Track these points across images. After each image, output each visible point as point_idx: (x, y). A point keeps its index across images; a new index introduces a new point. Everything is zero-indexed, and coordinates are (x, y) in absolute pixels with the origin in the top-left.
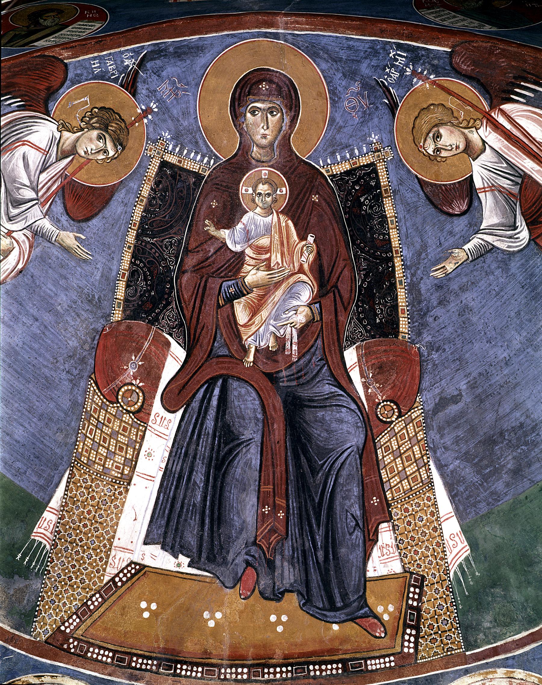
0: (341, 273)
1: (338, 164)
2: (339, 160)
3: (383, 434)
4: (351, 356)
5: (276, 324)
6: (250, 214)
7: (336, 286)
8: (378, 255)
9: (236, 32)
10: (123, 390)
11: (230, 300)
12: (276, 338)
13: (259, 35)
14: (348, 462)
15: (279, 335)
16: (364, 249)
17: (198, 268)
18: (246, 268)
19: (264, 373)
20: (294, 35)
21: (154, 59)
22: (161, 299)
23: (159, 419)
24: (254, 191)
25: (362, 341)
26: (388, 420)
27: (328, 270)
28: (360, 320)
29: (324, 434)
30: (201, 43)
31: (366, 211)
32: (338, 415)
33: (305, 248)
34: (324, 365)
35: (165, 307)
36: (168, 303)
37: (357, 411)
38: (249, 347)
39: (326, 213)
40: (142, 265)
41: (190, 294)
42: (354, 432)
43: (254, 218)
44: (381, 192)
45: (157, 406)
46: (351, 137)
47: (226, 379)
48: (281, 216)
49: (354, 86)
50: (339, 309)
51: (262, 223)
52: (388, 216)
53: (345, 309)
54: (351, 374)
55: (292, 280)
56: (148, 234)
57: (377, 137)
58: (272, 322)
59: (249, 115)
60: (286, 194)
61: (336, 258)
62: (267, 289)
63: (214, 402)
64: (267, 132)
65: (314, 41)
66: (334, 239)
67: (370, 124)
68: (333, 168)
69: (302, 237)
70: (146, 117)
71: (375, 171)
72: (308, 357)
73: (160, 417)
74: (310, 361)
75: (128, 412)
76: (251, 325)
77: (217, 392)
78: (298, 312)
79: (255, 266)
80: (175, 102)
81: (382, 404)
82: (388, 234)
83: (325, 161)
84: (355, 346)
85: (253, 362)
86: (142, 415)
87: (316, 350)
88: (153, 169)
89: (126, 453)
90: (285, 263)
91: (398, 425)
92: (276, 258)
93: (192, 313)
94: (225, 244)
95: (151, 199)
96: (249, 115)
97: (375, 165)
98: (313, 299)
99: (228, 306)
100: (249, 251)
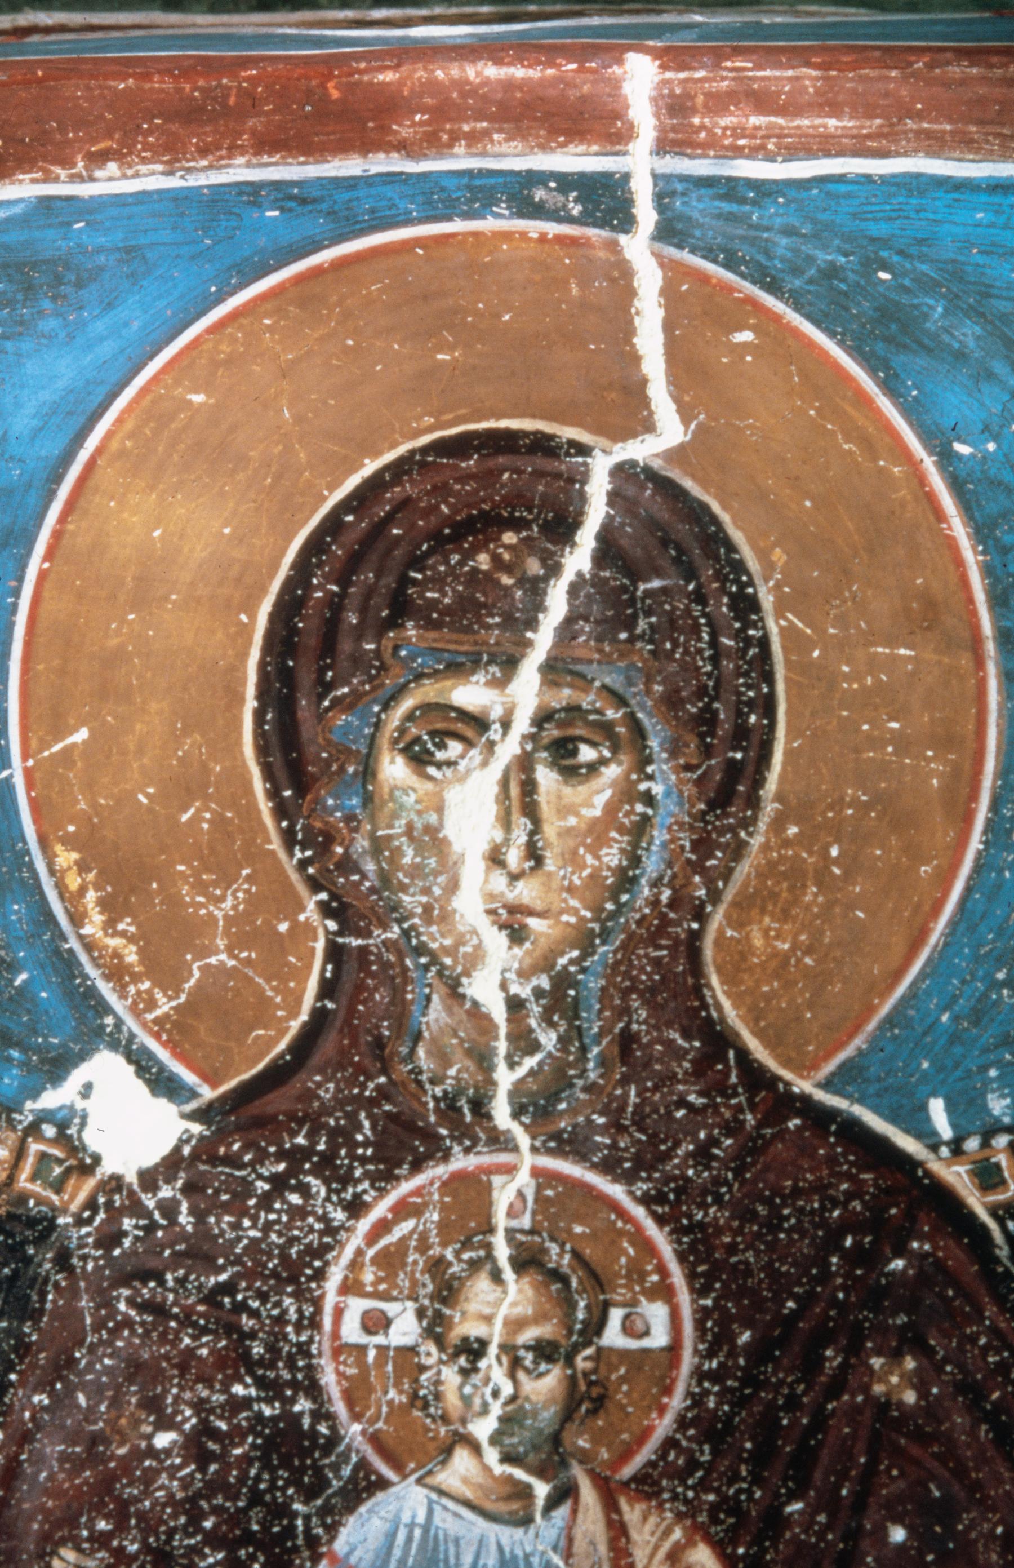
6: (406, 1501)
9: (312, 171)
13: (480, 192)
20: (730, 189)
24: (435, 1328)
30: (51, 242)
48: (631, 1513)
59: (394, 769)
60: (674, 1349)
64: (526, 892)
65: (875, 229)
83: (965, 1106)
96: (394, 769)
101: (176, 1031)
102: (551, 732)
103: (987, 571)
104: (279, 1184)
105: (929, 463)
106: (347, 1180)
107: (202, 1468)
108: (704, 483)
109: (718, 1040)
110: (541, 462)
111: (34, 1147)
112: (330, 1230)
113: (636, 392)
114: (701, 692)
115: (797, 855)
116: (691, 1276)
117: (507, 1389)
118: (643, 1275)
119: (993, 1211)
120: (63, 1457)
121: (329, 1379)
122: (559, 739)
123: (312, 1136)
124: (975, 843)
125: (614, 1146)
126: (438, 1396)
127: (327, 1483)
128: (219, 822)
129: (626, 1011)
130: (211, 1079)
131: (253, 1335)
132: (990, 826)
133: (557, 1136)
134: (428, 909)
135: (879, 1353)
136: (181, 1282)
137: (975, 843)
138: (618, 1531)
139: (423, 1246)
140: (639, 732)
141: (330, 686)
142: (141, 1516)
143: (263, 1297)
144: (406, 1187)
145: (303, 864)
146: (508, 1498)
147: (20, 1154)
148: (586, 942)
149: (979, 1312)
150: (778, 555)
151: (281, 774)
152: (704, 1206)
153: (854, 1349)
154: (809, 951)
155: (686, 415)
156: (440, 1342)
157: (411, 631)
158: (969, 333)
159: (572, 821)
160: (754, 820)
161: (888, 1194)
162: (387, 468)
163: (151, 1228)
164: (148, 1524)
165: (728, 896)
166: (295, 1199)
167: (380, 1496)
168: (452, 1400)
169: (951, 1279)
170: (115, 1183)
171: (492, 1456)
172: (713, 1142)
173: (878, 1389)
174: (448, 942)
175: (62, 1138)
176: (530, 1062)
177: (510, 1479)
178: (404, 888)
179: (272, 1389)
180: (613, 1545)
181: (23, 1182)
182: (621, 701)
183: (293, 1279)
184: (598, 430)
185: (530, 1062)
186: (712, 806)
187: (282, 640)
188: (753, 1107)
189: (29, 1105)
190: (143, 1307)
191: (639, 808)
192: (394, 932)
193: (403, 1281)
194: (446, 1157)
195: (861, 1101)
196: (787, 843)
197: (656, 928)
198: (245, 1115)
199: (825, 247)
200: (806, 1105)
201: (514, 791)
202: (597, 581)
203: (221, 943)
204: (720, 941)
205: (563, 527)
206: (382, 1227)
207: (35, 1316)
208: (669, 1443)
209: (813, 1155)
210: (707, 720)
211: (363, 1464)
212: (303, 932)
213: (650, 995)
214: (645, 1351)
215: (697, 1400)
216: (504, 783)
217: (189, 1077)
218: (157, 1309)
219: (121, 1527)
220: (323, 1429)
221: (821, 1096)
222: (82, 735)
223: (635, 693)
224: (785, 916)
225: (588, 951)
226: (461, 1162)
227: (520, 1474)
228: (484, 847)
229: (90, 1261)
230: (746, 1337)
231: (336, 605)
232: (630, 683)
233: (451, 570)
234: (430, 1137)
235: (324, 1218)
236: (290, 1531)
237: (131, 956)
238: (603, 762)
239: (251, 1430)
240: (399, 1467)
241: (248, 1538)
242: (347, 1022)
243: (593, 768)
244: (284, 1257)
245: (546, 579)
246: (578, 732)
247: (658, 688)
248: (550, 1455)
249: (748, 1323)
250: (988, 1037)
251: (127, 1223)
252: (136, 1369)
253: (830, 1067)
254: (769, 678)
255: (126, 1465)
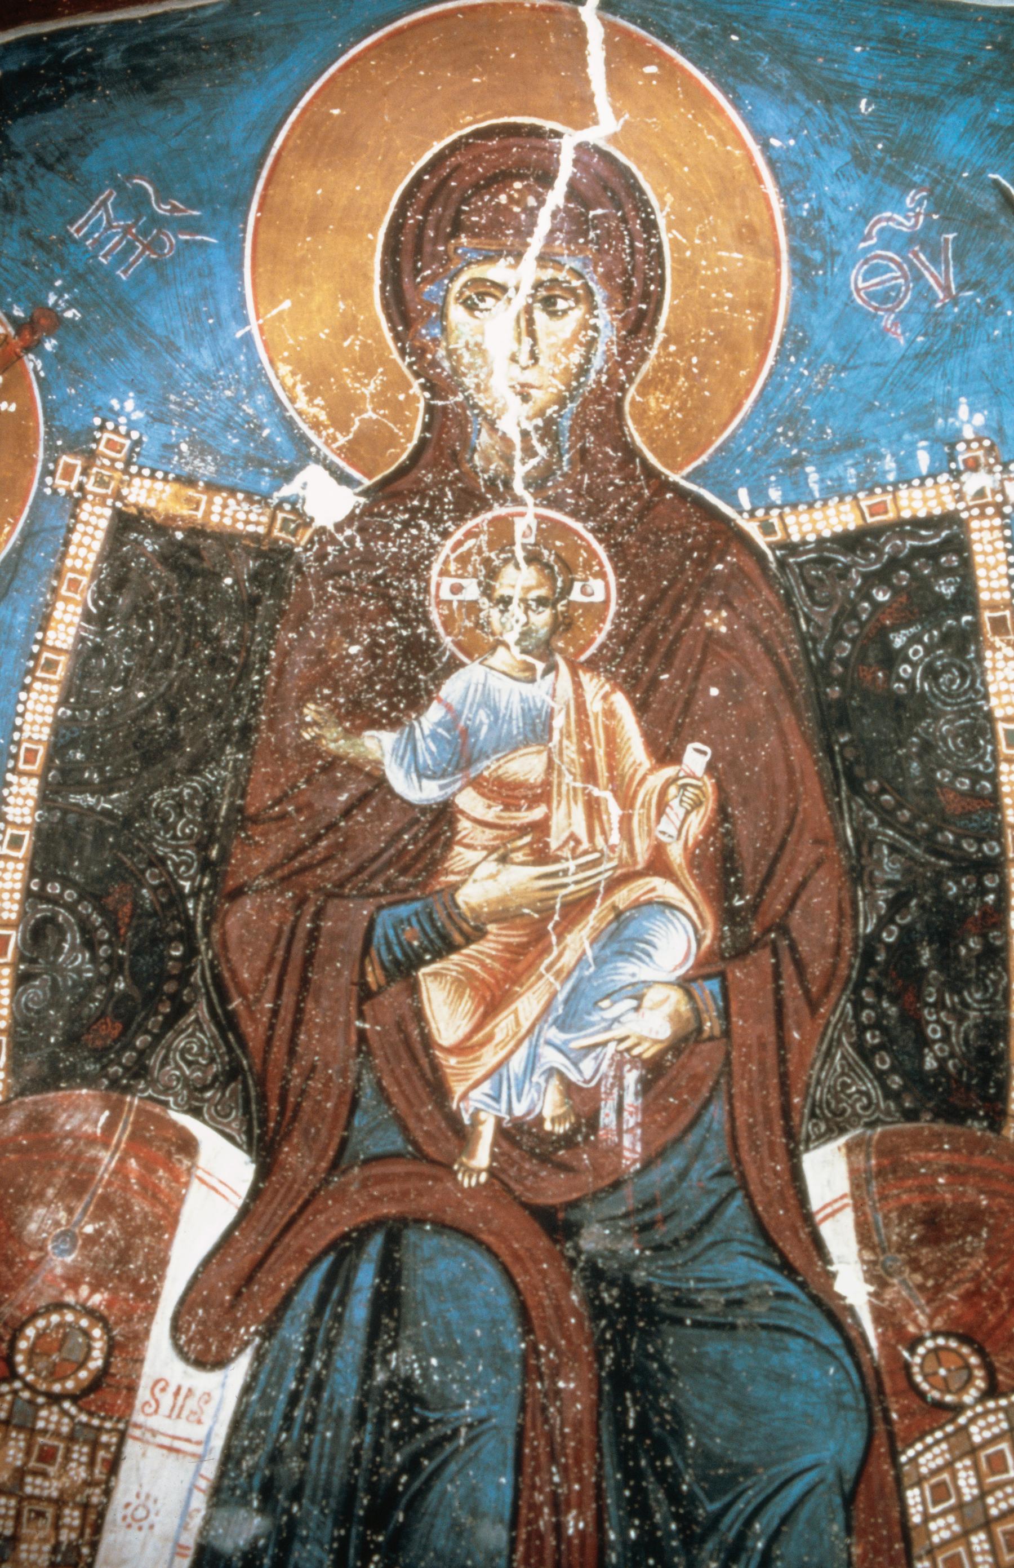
0: (802, 886)
1: (811, 506)
2: (815, 488)
3: (929, 1440)
4: (827, 1172)
5: (566, 1042)
7: (783, 930)
8: (946, 844)
10: (30, 1332)
11: (404, 969)
12: (569, 1089)
14: (804, 1513)
15: (574, 1076)
16: (891, 812)
17: (288, 873)
18: (461, 857)
19: (525, 1206)
21: (45, 105)
22: (151, 999)
23: (166, 1400)
24: (487, 591)
25: (871, 1125)
26: (949, 1398)
27: (755, 870)
28: (866, 1053)
29: (728, 1417)
31: (910, 682)
32: (775, 1359)
33: (673, 790)
34: (731, 1194)
35: (170, 1022)
36: (181, 1009)
37: (841, 1352)
38: (476, 1121)
39: (753, 673)
40: (70, 895)
41: (259, 964)
42: (826, 1421)
43: (485, 687)
44: (976, 627)
45: (160, 1356)
46: (870, 408)
47: (394, 1232)
49: (898, 205)
50: (790, 1005)
51: (516, 699)
52: (998, 713)
53: (813, 1005)
54: (827, 1231)
55: (623, 897)
56: (89, 782)
57: (979, 419)
58: (553, 1033)
60: (606, 602)
61: (788, 831)
62: (534, 931)
63: (359, 1311)
64: (530, 376)
66: (781, 766)
67: (954, 365)
68: (790, 520)
69: (665, 753)
70: (34, 347)
71: (959, 545)
72: (676, 1163)
73: (172, 1389)
74: (683, 1175)
75: (55, 1399)
76: (482, 1044)
77: (366, 1277)
78: (647, 1002)
79: (492, 850)
80: (152, 277)
81: (930, 1344)
82: (993, 777)
83: (758, 493)
84: (842, 1140)
85: (491, 1171)
86: (106, 1395)
87: (704, 1139)
88: (87, 544)
89: (57, 1527)
90: (599, 841)
91: (981, 1423)
92: (567, 820)
93: (272, 1027)
94: (381, 782)
95: (86, 658)
96: (456, 313)
97: (963, 524)
98: (699, 964)
99: (394, 988)
100: (469, 802)
101: (349, 452)
102: (543, 293)
103: (786, 213)
104: (406, 525)
105: (755, 149)
106: (440, 521)
107: (374, 662)
108: (628, 154)
109: (631, 453)
110: (534, 141)
111: (280, 516)
112: (433, 546)
113: (587, 102)
114: (625, 272)
115: (674, 363)
116: (615, 568)
117: (523, 619)
118: (591, 567)
119: (770, 545)
120: (306, 662)
121: (435, 617)
122: (547, 296)
123: (422, 501)
124: (770, 361)
125: (576, 504)
126: (489, 623)
127: (434, 665)
128: (364, 346)
129: (582, 437)
130: (369, 475)
131: (396, 598)
132: (779, 353)
133: (547, 498)
134: (478, 386)
135: (708, 607)
136: (359, 576)
137: (770, 361)
138: (578, 685)
139: (480, 552)
140: (590, 293)
141: (418, 271)
142: (346, 686)
143: (400, 580)
144: (470, 524)
145: (410, 365)
146: (524, 670)
147: (273, 518)
148: (561, 402)
149: (760, 592)
150: (669, 198)
151: (396, 318)
152: (622, 535)
153: (696, 605)
154: (679, 410)
155: (618, 114)
156: (490, 598)
157: (464, 239)
158: (782, 75)
159: (553, 340)
160: (652, 342)
161: (715, 533)
162: (447, 147)
163: (342, 550)
164: (349, 689)
165: (638, 380)
166: (414, 531)
167: (461, 671)
168: (496, 626)
169: (747, 576)
170: (322, 531)
171: (516, 650)
172: (627, 503)
173: (708, 624)
174: (489, 402)
175: (294, 510)
176: (533, 462)
177: (525, 662)
178: (464, 375)
179: (406, 623)
180: (575, 691)
181: (276, 533)
182: (580, 276)
183: (415, 571)
184: (569, 123)
185: (533, 462)
186: (630, 332)
187: (392, 248)
188: (648, 487)
189: (276, 495)
190: (340, 589)
191: (590, 333)
192: (460, 398)
193: (470, 568)
194: (490, 508)
195: (704, 487)
196: (669, 355)
197: (599, 395)
198: (388, 491)
199: (701, 18)
200: (675, 487)
201: (523, 324)
202: (566, 210)
203: (369, 407)
204: (633, 402)
205: (546, 178)
206: (459, 544)
207: (287, 597)
208: (603, 646)
209: (678, 511)
210: (628, 287)
211: (453, 656)
212: (412, 399)
213: (595, 429)
214: (592, 604)
215: (617, 626)
216: (518, 320)
217: (357, 475)
218: (347, 589)
219: (336, 692)
220: (432, 640)
221: (684, 483)
222: (287, 304)
223: (588, 273)
224: (668, 392)
225: (562, 404)
226: (498, 511)
227: (529, 659)
228: (509, 354)
229: (312, 568)
230: (642, 597)
231: (421, 227)
232: (585, 266)
233: (485, 205)
234: (482, 499)
235: (430, 541)
236: (417, 688)
237: (323, 417)
238: (571, 308)
239: (397, 643)
240: (470, 656)
241: (398, 692)
242: (438, 443)
243: (565, 312)
244: (410, 559)
245: (538, 208)
246: (557, 292)
247: (601, 270)
248: (545, 650)
249: (644, 591)
250: (771, 460)
251: (330, 549)
252: (339, 618)
253: (689, 469)
254: (661, 265)
255: (337, 663)
